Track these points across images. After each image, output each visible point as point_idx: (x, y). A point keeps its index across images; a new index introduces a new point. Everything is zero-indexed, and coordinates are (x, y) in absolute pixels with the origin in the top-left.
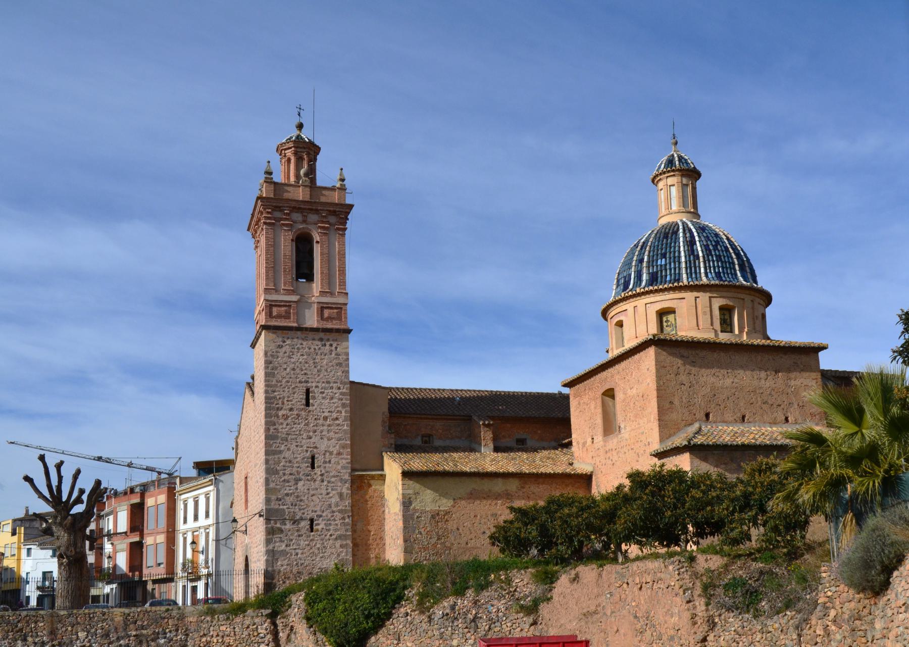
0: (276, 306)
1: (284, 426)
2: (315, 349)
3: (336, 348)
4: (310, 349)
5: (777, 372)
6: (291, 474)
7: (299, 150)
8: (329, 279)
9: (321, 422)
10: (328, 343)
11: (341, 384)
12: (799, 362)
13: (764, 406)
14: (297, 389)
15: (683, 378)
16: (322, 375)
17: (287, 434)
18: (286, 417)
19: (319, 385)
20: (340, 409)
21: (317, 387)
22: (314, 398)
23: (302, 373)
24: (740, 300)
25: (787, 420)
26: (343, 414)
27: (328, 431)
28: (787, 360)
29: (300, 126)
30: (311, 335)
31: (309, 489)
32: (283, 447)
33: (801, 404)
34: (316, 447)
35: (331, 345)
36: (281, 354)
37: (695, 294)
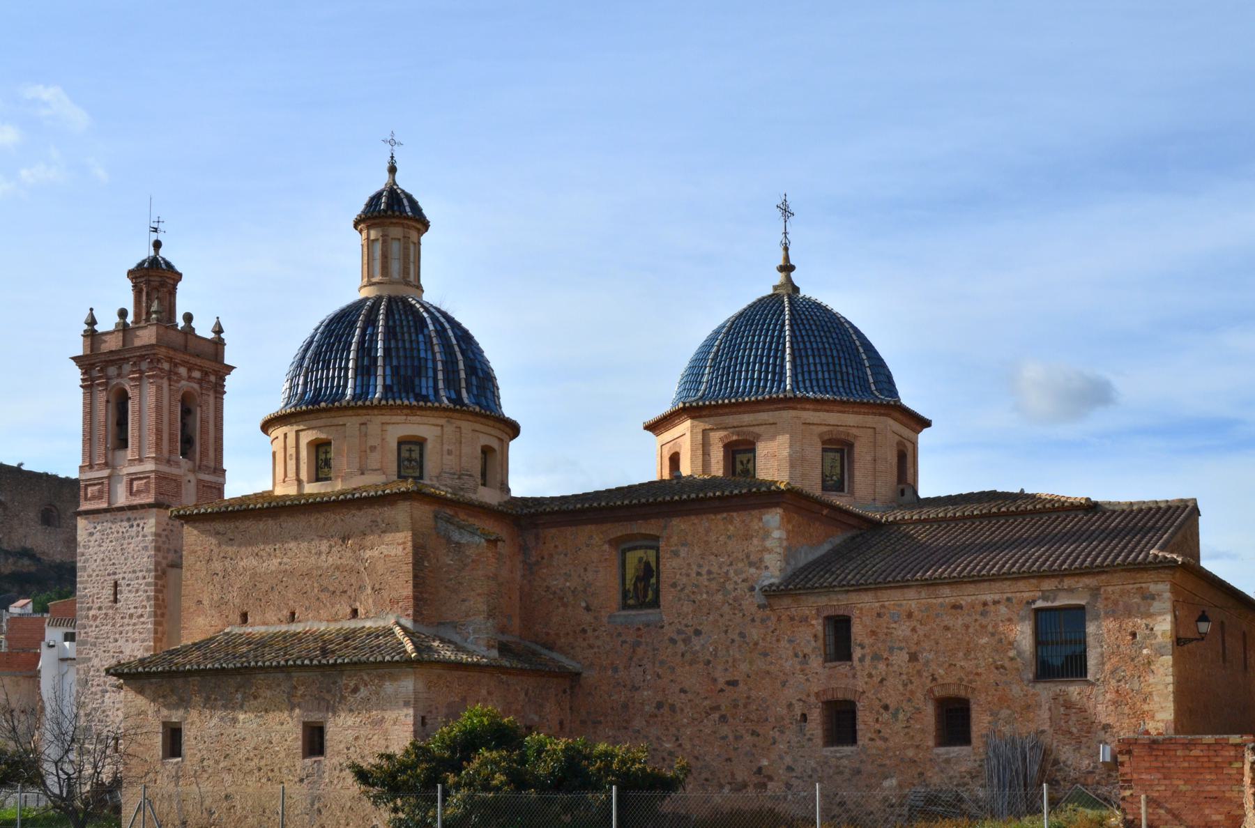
0: (91, 485)
1: (94, 629)
2: (123, 532)
3: (143, 528)
4: (118, 532)
5: (344, 539)
6: (98, 685)
7: (138, 281)
8: (140, 442)
9: (126, 621)
10: (135, 523)
11: (147, 572)
12: (379, 520)
13: (322, 596)
14: (105, 583)
15: (217, 565)
16: (129, 564)
17: (96, 638)
18: (95, 618)
19: (126, 575)
20: (143, 603)
21: (124, 578)
22: (121, 592)
23: (111, 563)
24: (339, 428)
25: (355, 613)
26: (148, 609)
27: (134, 631)
28: (361, 518)
29: (157, 245)
30: (119, 515)
31: (114, 703)
32: (92, 654)
33: (377, 586)
34: (121, 652)
35: (138, 525)
36: (92, 544)
37: (285, 429)
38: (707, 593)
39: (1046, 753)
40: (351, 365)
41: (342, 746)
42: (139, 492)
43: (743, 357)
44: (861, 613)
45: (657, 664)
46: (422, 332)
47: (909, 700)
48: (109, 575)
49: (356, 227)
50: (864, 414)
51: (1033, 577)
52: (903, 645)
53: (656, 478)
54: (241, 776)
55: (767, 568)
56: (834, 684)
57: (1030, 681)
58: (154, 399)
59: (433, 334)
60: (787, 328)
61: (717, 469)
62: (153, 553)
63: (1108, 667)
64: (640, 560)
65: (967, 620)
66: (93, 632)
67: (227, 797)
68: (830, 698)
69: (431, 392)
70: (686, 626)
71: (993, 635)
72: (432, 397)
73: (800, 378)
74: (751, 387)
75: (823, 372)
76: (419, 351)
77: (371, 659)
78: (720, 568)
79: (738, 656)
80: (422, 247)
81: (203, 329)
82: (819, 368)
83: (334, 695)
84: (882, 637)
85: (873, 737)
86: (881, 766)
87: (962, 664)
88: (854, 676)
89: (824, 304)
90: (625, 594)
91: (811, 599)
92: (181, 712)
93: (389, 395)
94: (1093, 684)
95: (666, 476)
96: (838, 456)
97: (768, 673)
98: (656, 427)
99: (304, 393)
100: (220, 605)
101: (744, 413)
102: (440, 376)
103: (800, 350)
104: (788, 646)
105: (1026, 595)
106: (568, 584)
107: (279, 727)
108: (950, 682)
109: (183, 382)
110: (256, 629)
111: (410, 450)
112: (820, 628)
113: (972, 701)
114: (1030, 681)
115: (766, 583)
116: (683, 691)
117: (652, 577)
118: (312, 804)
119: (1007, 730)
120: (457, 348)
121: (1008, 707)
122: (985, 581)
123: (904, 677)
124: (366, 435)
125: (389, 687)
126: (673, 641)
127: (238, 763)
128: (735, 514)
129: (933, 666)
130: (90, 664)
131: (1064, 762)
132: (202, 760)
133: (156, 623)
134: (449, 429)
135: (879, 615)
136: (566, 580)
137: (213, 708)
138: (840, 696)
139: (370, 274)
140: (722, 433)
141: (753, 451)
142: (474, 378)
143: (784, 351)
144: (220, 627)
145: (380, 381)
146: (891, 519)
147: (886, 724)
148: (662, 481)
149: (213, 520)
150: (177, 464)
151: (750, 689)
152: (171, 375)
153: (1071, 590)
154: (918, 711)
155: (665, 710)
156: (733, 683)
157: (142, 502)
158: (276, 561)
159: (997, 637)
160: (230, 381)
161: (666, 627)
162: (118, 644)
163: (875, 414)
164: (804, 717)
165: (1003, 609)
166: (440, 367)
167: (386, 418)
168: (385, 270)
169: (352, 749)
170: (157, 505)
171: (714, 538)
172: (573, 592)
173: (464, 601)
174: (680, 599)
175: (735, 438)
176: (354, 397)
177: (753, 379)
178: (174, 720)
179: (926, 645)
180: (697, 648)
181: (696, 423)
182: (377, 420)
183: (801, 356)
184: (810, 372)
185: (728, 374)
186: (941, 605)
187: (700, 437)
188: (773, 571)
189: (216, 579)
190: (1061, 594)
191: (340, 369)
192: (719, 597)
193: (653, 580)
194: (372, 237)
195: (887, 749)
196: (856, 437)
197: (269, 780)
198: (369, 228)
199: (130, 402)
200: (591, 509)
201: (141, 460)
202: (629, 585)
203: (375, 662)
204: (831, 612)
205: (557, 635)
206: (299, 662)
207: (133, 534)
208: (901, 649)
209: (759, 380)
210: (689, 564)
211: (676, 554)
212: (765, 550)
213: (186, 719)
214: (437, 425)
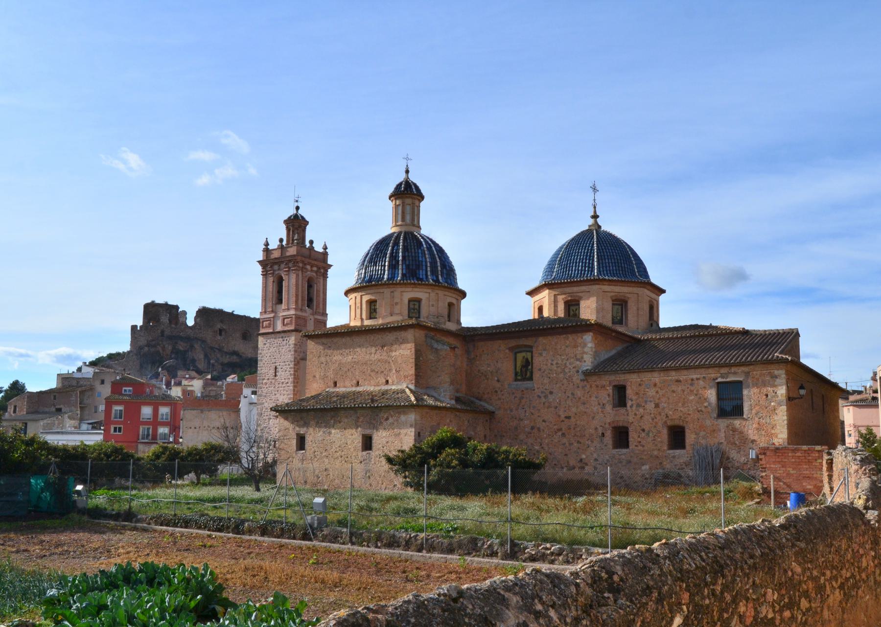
5: (383, 347)
13: (372, 374)
15: (323, 359)
18: (266, 384)
22: (278, 371)
25: (387, 382)
28: (390, 337)
32: (264, 401)
33: (398, 370)
38: (556, 373)
39: (723, 454)
40: (387, 264)
41: (380, 446)
42: (287, 324)
43: (574, 260)
44: (631, 384)
45: (531, 408)
46: (420, 248)
47: (655, 427)
48: (273, 363)
49: (390, 199)
50: (633, 287)
51: (716, 367)
52: (652, 399)
53: (532, 318)
54: (333, 460)
55: (585, 361)
56: (617, 418)
57: (715, 418)
58: (295, 280)
59: (425, 249)
60: (595, 245)
61: (561, 314)
62: (293, 353)
63: (754, 411)
64: (524, 357)
65: (684, 387)
66: (265, 391)
67: (326, 470)
68: (616, 425)
69: (424, 276)
70: (546, 389)
71: (696, 395)
72: (425, 279)
73: (601, 269)
74: (578, 274)
75: (613, 267)
76: (419, 257)
77: (395, 404)
78: (562, 361)
79: (571, 404)
80: (421, 208)
81: (318, 248)
82: (611, 265)
83: (377, 421)
84: (641, 395)
85: (637, 444)
86: (641, 459)
87: (681, 409)
88: (628, 415)
89: (613, 234)
90: (516, 374)
91: (607, 377)
92: (305, 429)
93: (405, 278)
94: (746, 420)
95: (536, 317)
96: (620, 307)
97: (585, 412)
98: (531, 293)
99: (365, 277)
100: (324, 378)
101: (574, 286)
102: (429, 269)
103: (601, 256)
104: (595, 399)
105: (712, 375)
106: (489, 369)
107: (350, 437)
108: (675, 418)
109: (309, 273)
110: (341, 390)
111: (414, 305)
112: (611, 391)
113: (686, 428)
114: (715, 418)
115: (585, 369)
116: (544, 421)
117: (529, 365)
118: (366, 474)
119: (703, 442)
120: (437, 256)
121: (704, 431)
122: (692, 368)
123: (652, 415)
124: (393, 297)
125: (403, 418)
126: (539, 397)
127: (331, 453)
128: (569, 335)
129: (666, 410)
130: (263, 406)
131: (732, 458)
132: (315, 452)
133: (295, 386)
134: (433, 295)
135: (640, 385)
136: (488, 367)
137: (320, 427)
138: (621, 424)
139: (396, 221)
140: (563, 296)
141: (579, 305)
142: (445, 270)
143: (594, 257)
144: (324, 388)
145: (400, 271)
146: (646, 338)
147: (643, 438)
148: (534, 319)
149: (322, 337)
150: (305, 311)
151: (577, 420)
152: (303, 269)
153: (735, 373)
154: (659, 432)
155: (535, 431)
156: (568, 418)
157: (289, 329)
158: (350, 357)
159: (698, 396)
160: (330, 272)
161: (536, 390)
162: (276, 396)
163: (638, 287)
164: (603, 434)
165: (701, 382)
166: (429, 265)
167: (403, 289)
168: (403, 219)
169: (385, 447)
170: (296, 330)
171: (559, 347)
172: (491, 372)
173: (439, 376)
174: (543, 376)
175: (570, 298)
176: (388, 279)
177: (578, 270)
178: (302, 432)
179: (664, 400)
180: (551, 400)
181: (551, 291)
182: (399, 290)
183: (602, 260)
184: (606, 267)
185: (567, 268)
186: (671, 380)
187: (553, 298)
188: (588, 363)
189: (323, 365)
190: (730, 375)
191: (382, 266)
192: (561, 376)
193: (530, 367)
194: (397, 204)
195: (644, 451)
196: (628, 298)
197: (346, 462)
198: (396, 199)
199: (284, 282)
200: (500, 333)
201: (288, 309)
202: (518, 369)
203: (396, 406)
204: (616, 383)
205: (484, 393)
206: (360, 405)
207: (284, 344)
208: (651, 401)
209: (582, 270)
210: (547, 360)
211: (541, 354)
212: (584, 353)
213: (307, 432)
214: (427, 293)
